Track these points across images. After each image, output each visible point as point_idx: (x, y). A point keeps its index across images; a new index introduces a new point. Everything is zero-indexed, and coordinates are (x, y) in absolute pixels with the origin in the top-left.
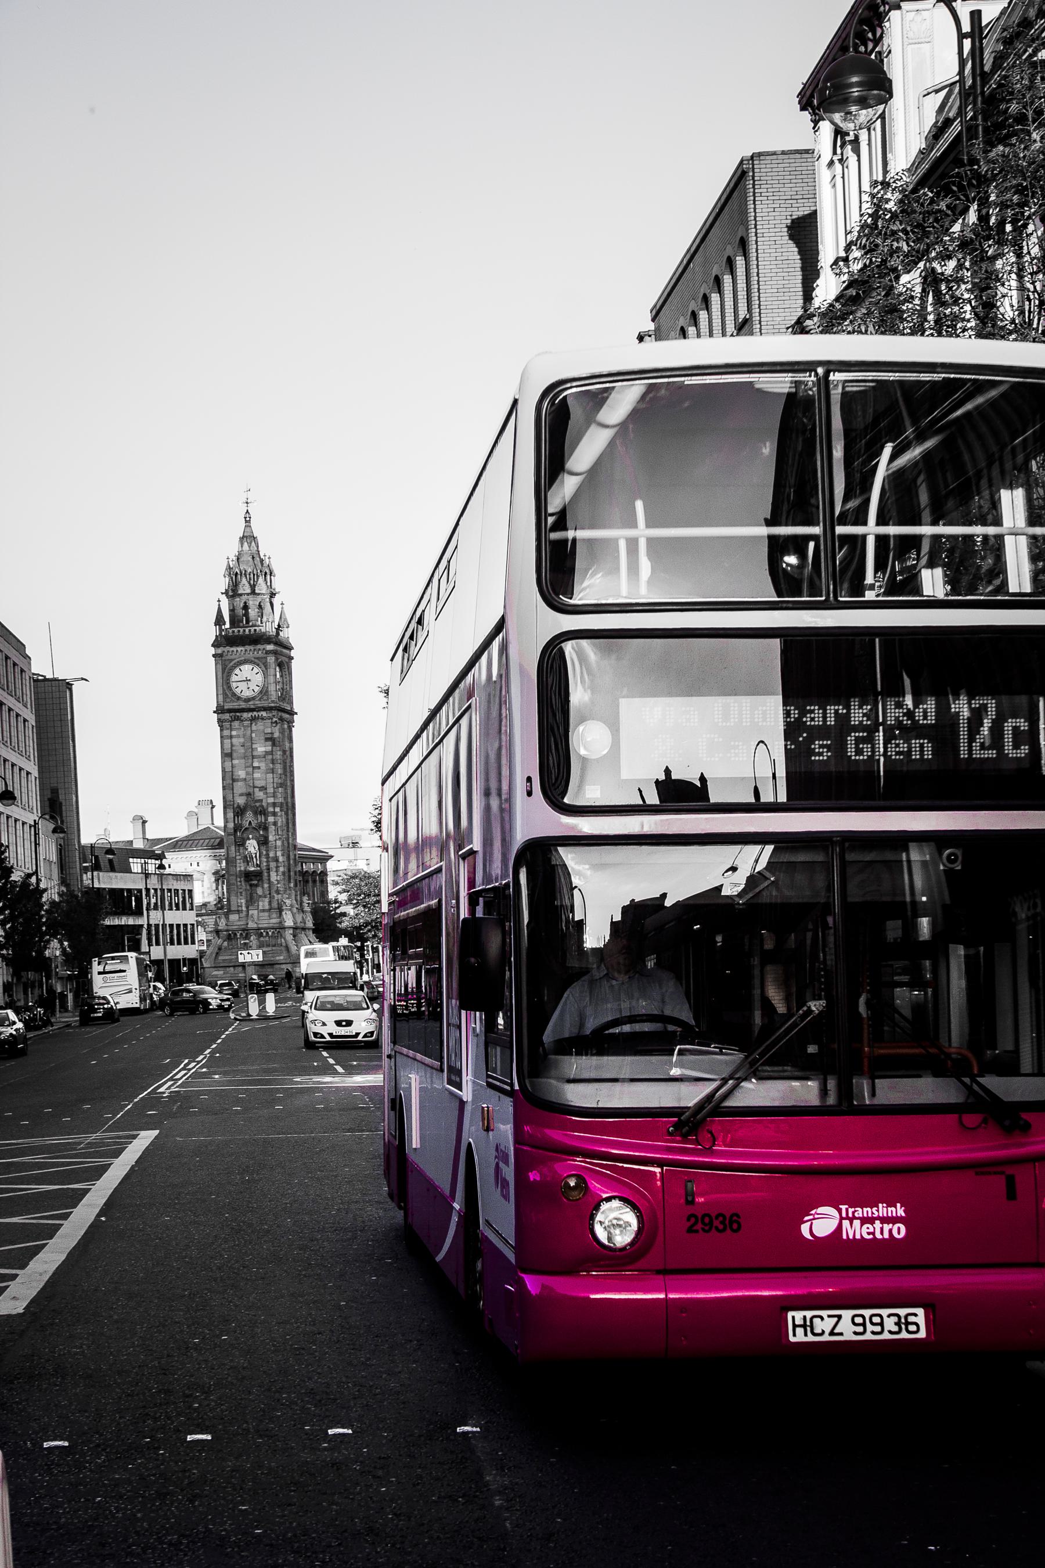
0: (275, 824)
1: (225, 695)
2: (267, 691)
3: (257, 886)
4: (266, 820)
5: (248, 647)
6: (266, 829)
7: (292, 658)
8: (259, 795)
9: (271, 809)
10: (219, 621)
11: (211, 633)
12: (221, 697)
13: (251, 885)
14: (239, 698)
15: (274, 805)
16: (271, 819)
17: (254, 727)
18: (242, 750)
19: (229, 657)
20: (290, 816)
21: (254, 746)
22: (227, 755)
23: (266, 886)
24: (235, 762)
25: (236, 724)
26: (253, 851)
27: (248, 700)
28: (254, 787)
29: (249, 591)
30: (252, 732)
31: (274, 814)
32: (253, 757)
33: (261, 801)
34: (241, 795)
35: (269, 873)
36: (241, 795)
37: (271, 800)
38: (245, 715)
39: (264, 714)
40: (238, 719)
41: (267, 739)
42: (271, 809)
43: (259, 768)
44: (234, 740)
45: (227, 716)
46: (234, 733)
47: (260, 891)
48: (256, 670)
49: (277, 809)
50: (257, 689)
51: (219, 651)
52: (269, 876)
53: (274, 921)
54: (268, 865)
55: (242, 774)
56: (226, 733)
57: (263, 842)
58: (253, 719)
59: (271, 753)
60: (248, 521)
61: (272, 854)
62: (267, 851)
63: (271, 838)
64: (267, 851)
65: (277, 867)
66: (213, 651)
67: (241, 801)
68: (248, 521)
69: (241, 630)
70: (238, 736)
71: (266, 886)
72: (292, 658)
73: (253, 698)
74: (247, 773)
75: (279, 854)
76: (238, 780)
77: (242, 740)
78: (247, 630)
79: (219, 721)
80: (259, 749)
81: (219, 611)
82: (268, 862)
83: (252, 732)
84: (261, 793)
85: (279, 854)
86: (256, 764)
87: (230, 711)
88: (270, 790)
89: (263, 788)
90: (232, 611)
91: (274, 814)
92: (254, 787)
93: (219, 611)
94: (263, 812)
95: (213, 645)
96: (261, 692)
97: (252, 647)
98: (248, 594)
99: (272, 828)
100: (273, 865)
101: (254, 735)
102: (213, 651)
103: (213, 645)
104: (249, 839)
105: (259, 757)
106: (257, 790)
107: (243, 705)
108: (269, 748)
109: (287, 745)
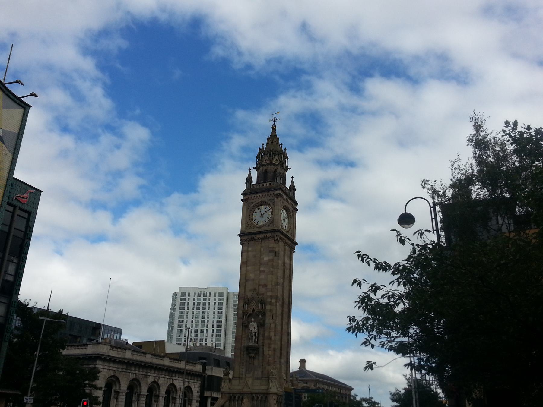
0: (271, 311)
1: (247, 225)
2: (273, 221)
3: (254, 358)
4: (265, 308)
5: (264, 194)
6: (264, 314)
7: (297, 210)
8: (262, 290)
9: (269, 300)
10: (249, 180)
11: (243, 187)
12: (244, 226)
13: (250, 357)
14: (255, 226)
15: (271, 297)
16: (268, 307)
17: (263, 244)
19: (252, 201)
20: (286, 310)
21: (262, 257)
22: (244, 263)
23: (261, 358)
24: (249, 268)
25: (252, 243)
26: (253, 330)
27: (259, 227)
28: (259, 285)
30: (261, 247)
31: (271, 304)
32: (261, 264)
33: (263, 294)
34: (250, 291)
36: (250, 291)
37: (269, 294)
39: (270, 235)
40: (253, 239)
41: (271, 251)
42: (269, 300)
43: (264, 271)
44: (250, 253)
45: (246, 238)
46: (250, 249)
47: (256, 362)
48: (268, 208)
49: (274, 301)
50: (267, 220)
51: (246, 197)
52: (263, 351)
53: (263, 387)
54: (263, 343)
55: (252, 276)
56: (245, 248)
57: (261, 325)
58: (263, 239)
59: (272, 260)
60: (274, 129)
61: (266, 334)
63: (267, 321)
64: (264, 331)
65: (270, 344)
66: (242, 197)
67: (249, 295)
68: (274, 129)
69: (261, 185)
71: (261, 358)
72: (297, 210)
73: (264, 226)
75: (272, 334)
78: (265, 184)
80: (265, 259)
81: (250, 174)
82: (264, 340)
83: (261, 247)
85: (272, 334)
86: (262, 269)
87: (248, 234)
88: (269, 286)
89: (265, 286)
90: (258, 177)
91: (271, 304)
92: (259, 285)
93: (250, 174)
94: (264, 303)
95: (242, 194)
96: (269, 221)
97: (266, 194)
98: (268, 164)
99: (268, 314)
100: (267, 342)
101: (262, 249)
102: (242, 197)
103: (242, 194)
104: (252, 322)
106: (261, 287)
107: (257, 230)
108: (271, 257)
109: (287, 261)
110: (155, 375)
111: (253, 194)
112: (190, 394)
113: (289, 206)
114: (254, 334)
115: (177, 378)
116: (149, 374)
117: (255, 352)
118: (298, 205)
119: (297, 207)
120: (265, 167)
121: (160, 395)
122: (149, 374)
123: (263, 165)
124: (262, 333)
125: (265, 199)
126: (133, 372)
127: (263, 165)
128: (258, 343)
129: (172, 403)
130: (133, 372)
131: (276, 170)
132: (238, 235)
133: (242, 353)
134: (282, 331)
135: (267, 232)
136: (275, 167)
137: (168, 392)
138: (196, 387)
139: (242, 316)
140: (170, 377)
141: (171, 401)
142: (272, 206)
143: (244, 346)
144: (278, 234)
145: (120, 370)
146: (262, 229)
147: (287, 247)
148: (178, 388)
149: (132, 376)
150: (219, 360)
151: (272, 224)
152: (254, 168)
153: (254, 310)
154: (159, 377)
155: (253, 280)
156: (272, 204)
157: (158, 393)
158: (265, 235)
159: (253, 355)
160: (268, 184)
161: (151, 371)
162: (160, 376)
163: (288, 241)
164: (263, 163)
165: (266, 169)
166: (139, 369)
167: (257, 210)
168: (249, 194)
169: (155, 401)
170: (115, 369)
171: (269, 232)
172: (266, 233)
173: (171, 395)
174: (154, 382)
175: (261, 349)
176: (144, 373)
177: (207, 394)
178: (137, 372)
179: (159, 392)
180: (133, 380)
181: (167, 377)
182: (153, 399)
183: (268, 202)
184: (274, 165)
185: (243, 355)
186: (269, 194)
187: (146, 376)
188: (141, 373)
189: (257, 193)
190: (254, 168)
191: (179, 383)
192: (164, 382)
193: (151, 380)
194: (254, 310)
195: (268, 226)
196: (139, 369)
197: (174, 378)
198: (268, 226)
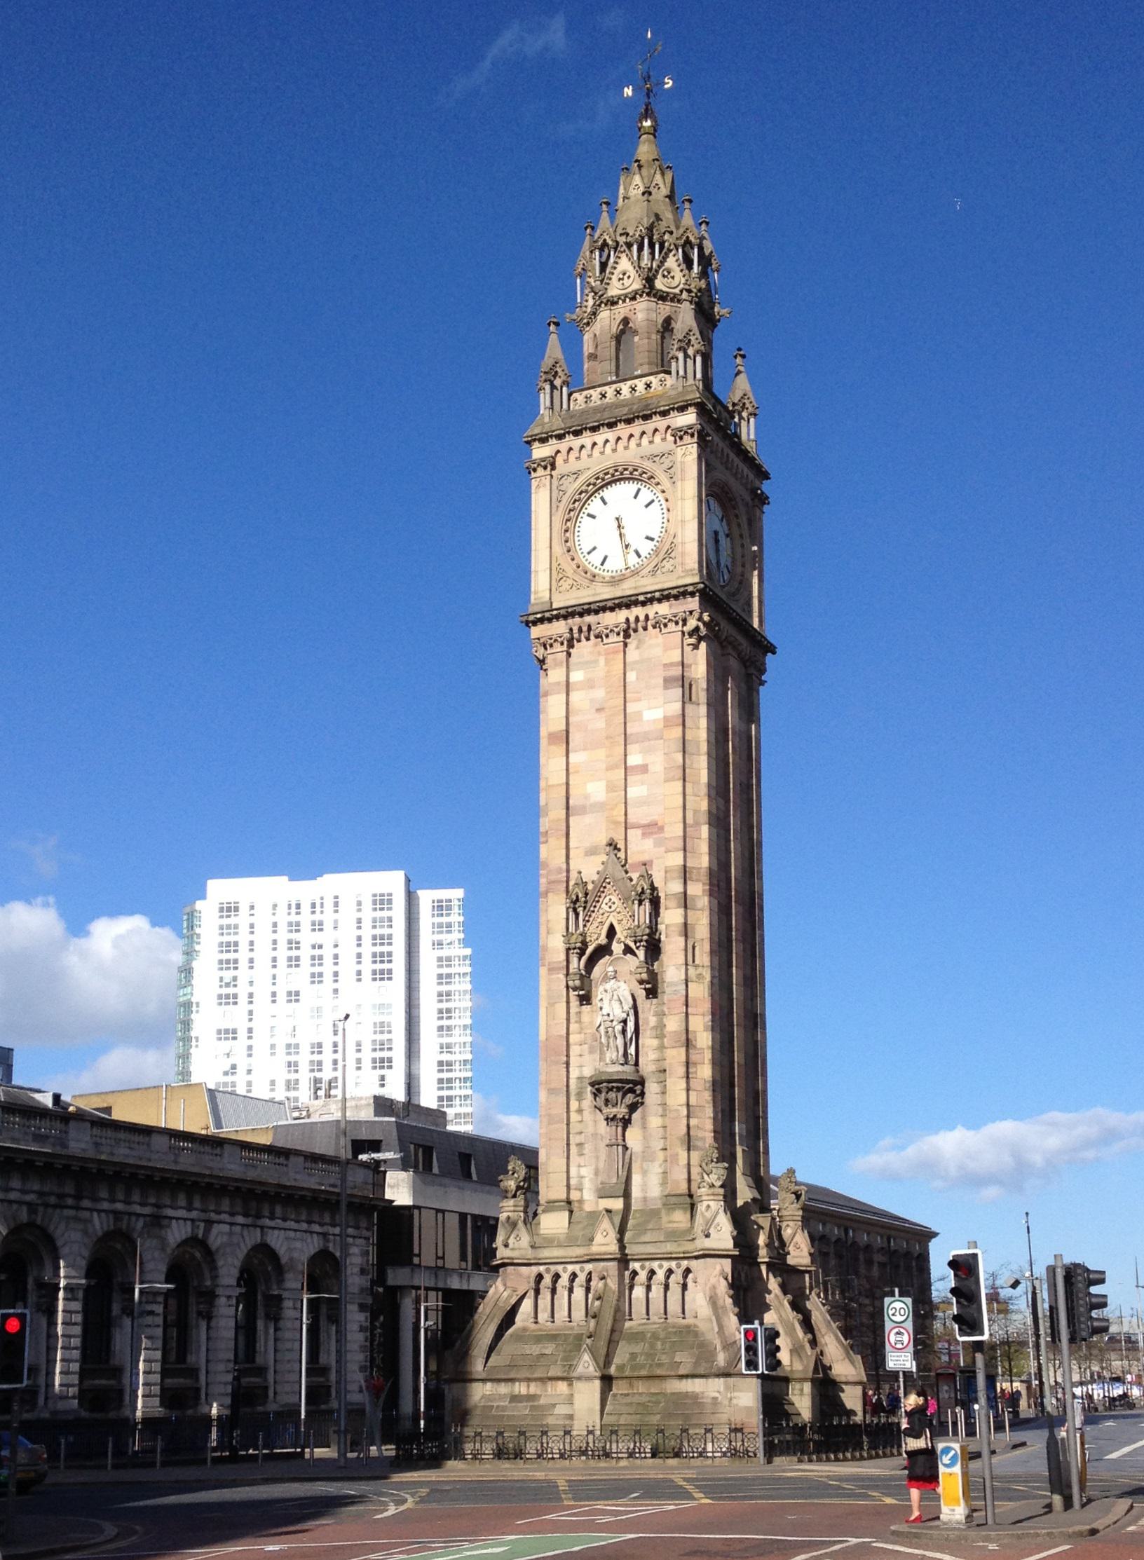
5: (623, 430)
17: (633, 653)
18: (599, 723)
19: (573, 465)
23: (655, 1122)
27: (615, 581)
29: (637, 285)
34: (591, 852)
35: (662, 1082)
36: (591, 852)
38: (609, 619)
39: (663, 609)
41: (668, 682)
43: (644, 769)
48: (646, 494)
50: (646, 548)
54: (661, 1059)
62: (661, 1015)
64: (661, 1015)
69: (610, 391)
70: (590, 684)
72: (763, 500)
74: (610, 788)
76: (583, 810)
77: (600, 693)
78: (625, 388)
82: (662, 1047)
84: (648, 843)
87: (567, 613)
89: (652, 828)
96: (656, 551)
101: (631, 676)
105: (645, 737)
107: (605, 593)
110: (194, 1214)
111: (577, 433)
113: (732, 482)
114: (619, 1027)
115: (279, 1223)
116: (170, 1212)
117: (630, 1098)
118: (766, 476)
119: (766, 487)
120: (622, 310)
121: (219, 1291)
122: (170, 1212)
123: (612, 302)
124: (653, 1021)
125: (629, 454)
126: (105, 1205)
127: (612, 302)
130: (105, 1205)
131: (668, 322)
133: (574, 1105)
136: (665, 309)
137: (248, 1276)
139: (563, 957)
140: (249, 1221)
141: (261, 1311)
142: (666, 484)
143: (580, 1079)
145: (53, 1200)
146: (627, 589)
147: (734, 663)
148: (284, 1260)
149: (99, 1224)
151: (668, 565)
153: (611, 932)
154: (209, 1223)
155: (600, 807)
156: (662, 477)
157: (208, 1283)
158: (639, 611)
159: (621, 1111)
160: (640, 384)
161: (174, 1197)
162: (213, 1216)
163: (740, 639)
164: (613, 291)
165: (626, 321)
166: (128, 1193)
167: (595, 506)
168: (560, 437)
169: (199, 1313)
170: (30, 1197)
171: (660, 601)
172: (644, 604)
173: (261, 1288)
174: (193, 1241)
175: (652, 1088)
176: (147, 1210)
178: (119, 1206)
179: (215, 1277)
180: (108, 1236)
181: (240, 1219)
182: (193, 1309)
183: (647, 465)
184: (663, 297)
185: (580, 1111)
186: (649, 426)
187: (157, 1222)
188: (138, 1209)
189: (594, 429)
191: (295, 1244)
192: (231, 1241)
193: (177, 1233)
194: (611, 932)
195: (654, 572)
196: (128, 1193)
197: (267, 1222)
198: (654, 572)
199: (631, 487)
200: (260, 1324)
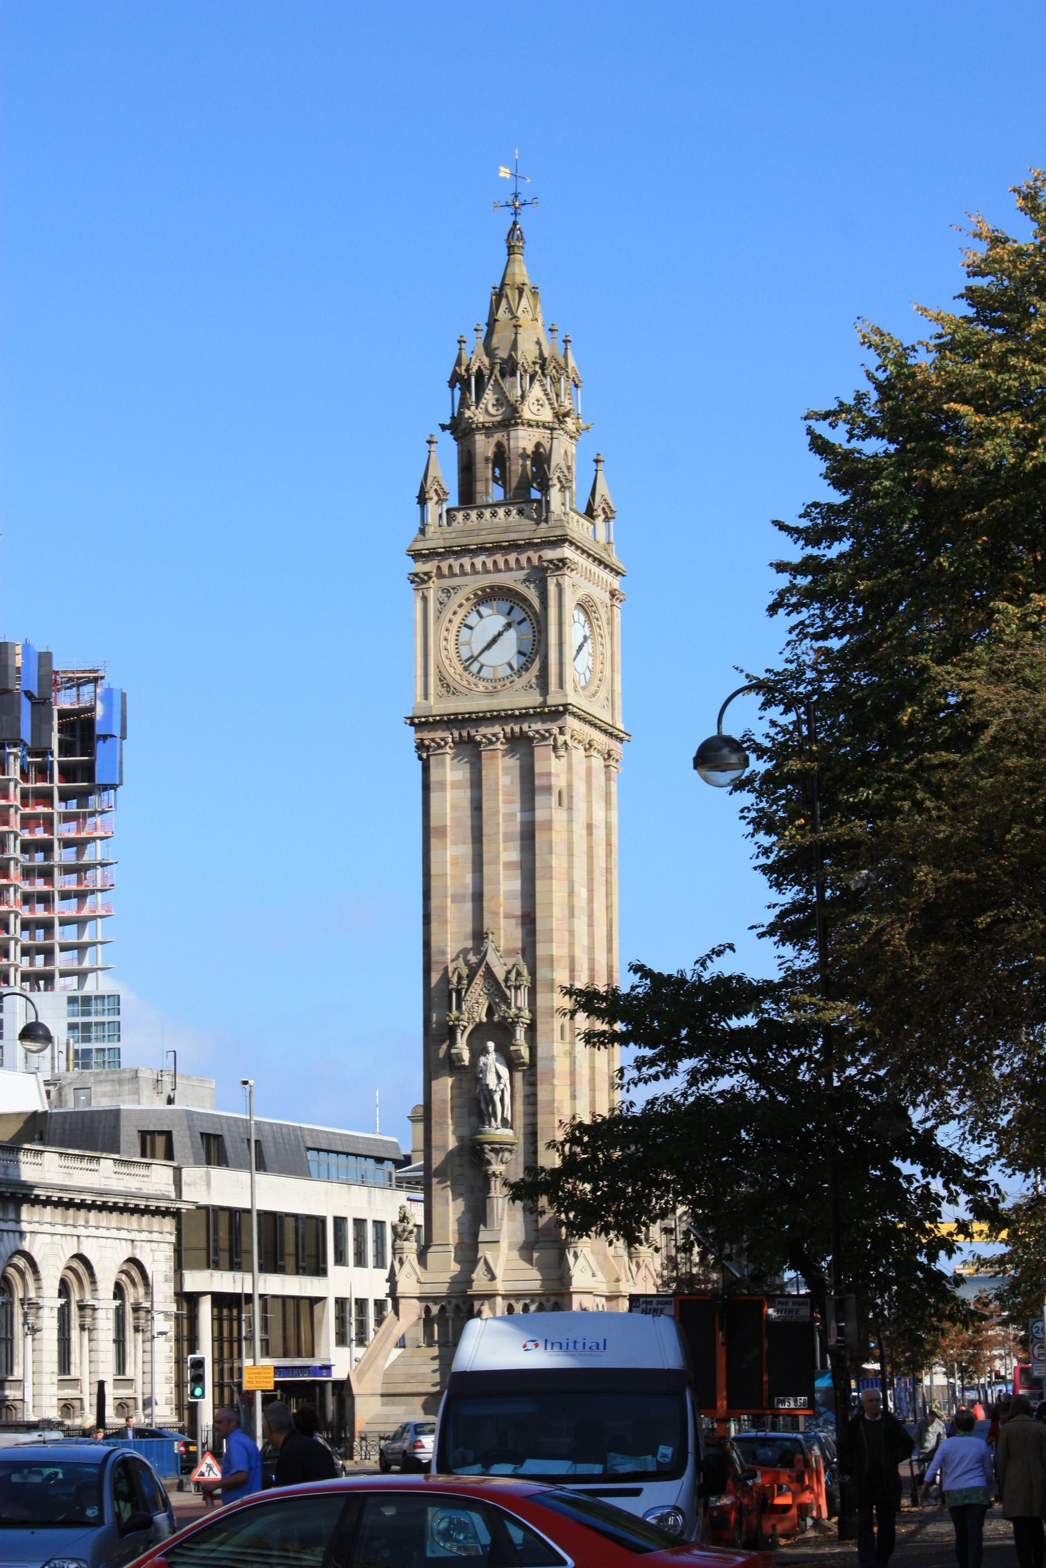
6: (531, 1028)
79: (421, 746)
112: (141, 1290)
128: (511, 1128)
129: (82, 1328)
132: (412, 721)
134: (592, 1080)
135: (524, 716)
138: (159, 1261)
144: (571, 722)
146: (505, 702)
150: (218, 1138)
152: (444, 427)
173: (75, 1296)
177: (196, 1281)
179: (39, 1288)
190: (444, 427)
199: (506, 606)
200: (75, 1333)
